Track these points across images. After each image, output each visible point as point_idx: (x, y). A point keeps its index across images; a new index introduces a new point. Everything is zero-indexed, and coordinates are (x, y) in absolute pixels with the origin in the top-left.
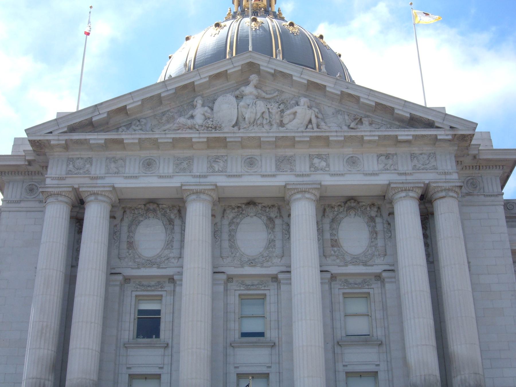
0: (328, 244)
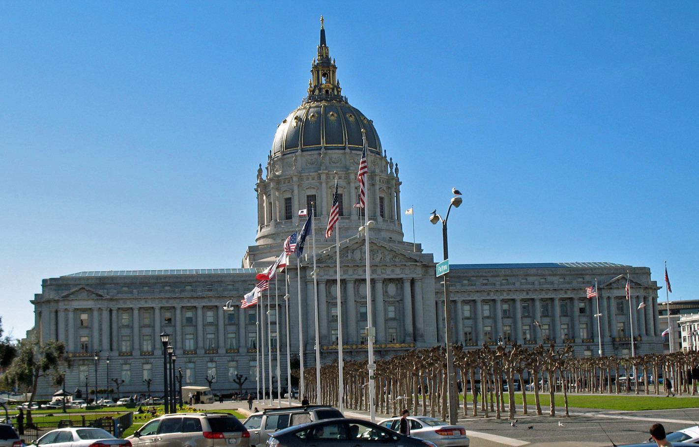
0: (385, 292)
